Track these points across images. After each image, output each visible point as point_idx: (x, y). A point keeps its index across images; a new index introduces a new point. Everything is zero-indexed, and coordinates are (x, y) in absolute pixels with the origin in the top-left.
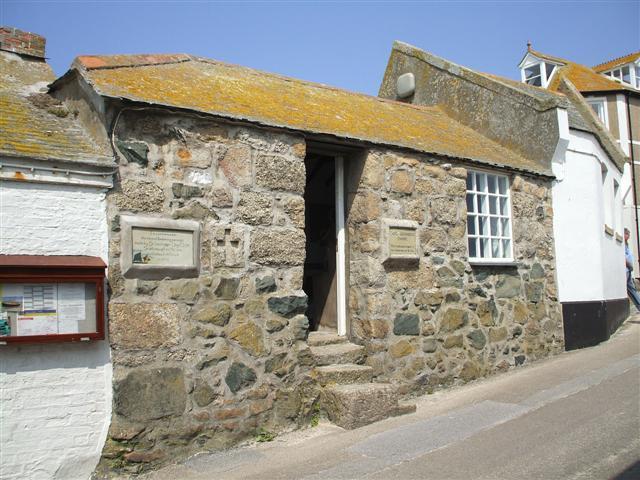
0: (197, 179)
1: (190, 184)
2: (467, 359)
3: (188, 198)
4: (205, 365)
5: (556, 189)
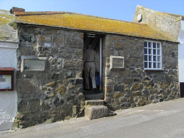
1: (44, 47)
5: (179, 45)
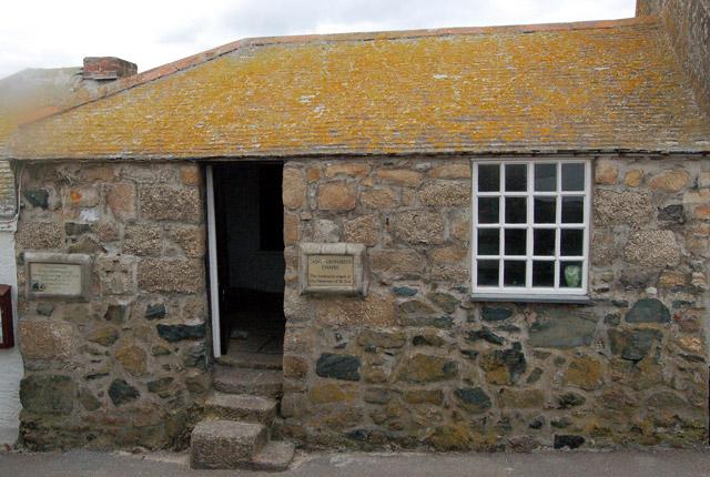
0: (89, 216)
2: (447, 422)
3: (79, 233)
4: (90, 377)
